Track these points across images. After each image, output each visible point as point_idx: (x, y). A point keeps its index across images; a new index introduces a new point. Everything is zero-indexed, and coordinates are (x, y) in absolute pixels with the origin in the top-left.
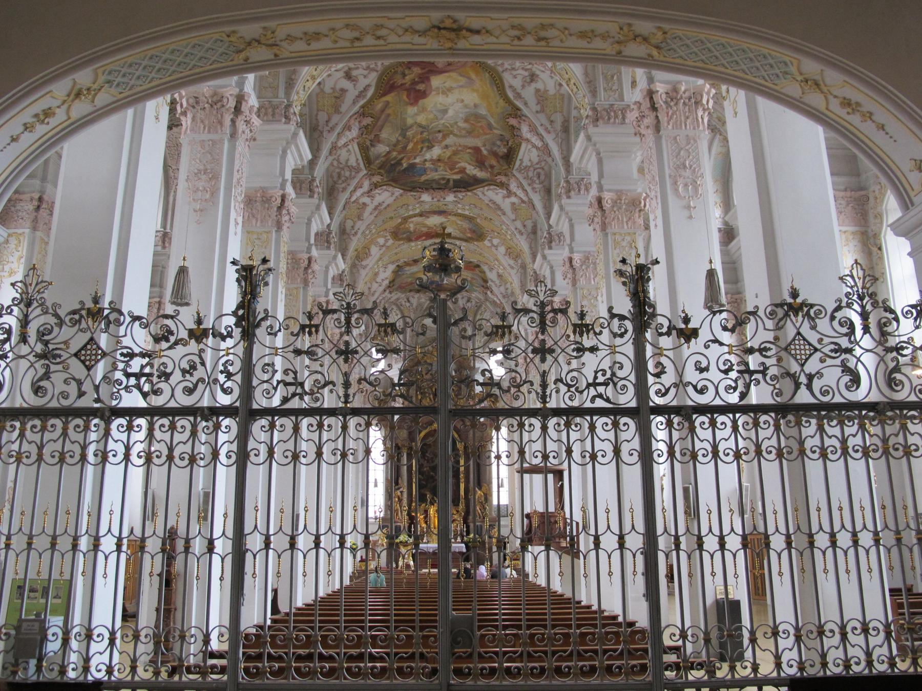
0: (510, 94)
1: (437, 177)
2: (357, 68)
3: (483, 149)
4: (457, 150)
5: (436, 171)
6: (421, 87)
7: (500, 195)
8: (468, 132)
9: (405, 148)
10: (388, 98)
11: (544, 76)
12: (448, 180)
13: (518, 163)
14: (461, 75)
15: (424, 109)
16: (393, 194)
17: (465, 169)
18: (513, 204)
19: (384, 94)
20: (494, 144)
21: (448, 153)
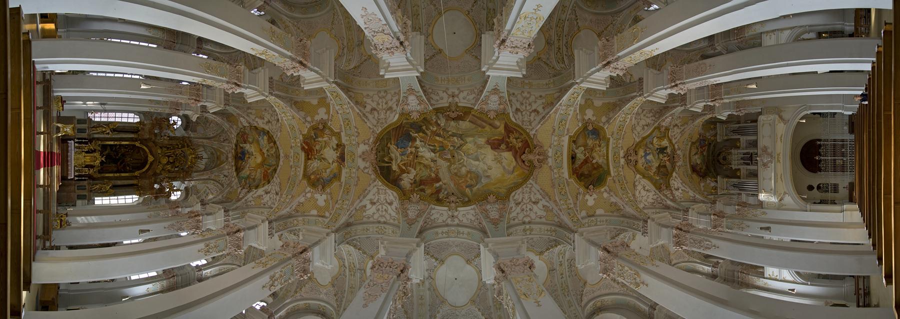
0: (513, 194)
1: (393, 155)
2: (522, 116)
3: (441, 183)
4: (430, 168)
5: (401, 155)
6: (503, 146)
7: (373, 197)
8: (456, 174)
9: (439, 135)
10: (502, 129)
11: (519, 209)
12: (391, 163)
13: (433, 206)
14: (514, 168)
15: (479, 147)
16: (375, 126)
17: (408, 173)
18: (365, 206)
19: (505, 127)
20: (446, 190)
21: (426, 162)
